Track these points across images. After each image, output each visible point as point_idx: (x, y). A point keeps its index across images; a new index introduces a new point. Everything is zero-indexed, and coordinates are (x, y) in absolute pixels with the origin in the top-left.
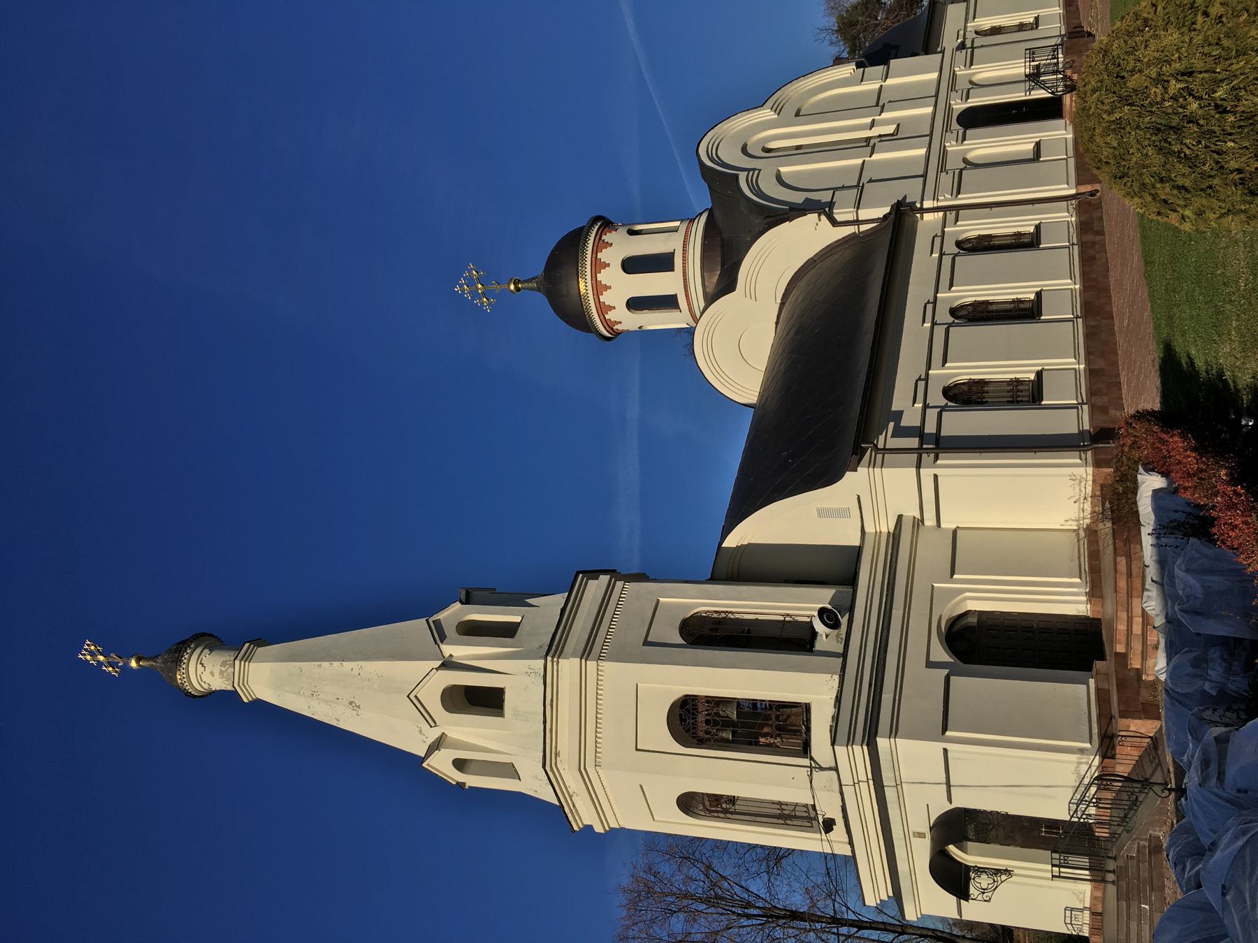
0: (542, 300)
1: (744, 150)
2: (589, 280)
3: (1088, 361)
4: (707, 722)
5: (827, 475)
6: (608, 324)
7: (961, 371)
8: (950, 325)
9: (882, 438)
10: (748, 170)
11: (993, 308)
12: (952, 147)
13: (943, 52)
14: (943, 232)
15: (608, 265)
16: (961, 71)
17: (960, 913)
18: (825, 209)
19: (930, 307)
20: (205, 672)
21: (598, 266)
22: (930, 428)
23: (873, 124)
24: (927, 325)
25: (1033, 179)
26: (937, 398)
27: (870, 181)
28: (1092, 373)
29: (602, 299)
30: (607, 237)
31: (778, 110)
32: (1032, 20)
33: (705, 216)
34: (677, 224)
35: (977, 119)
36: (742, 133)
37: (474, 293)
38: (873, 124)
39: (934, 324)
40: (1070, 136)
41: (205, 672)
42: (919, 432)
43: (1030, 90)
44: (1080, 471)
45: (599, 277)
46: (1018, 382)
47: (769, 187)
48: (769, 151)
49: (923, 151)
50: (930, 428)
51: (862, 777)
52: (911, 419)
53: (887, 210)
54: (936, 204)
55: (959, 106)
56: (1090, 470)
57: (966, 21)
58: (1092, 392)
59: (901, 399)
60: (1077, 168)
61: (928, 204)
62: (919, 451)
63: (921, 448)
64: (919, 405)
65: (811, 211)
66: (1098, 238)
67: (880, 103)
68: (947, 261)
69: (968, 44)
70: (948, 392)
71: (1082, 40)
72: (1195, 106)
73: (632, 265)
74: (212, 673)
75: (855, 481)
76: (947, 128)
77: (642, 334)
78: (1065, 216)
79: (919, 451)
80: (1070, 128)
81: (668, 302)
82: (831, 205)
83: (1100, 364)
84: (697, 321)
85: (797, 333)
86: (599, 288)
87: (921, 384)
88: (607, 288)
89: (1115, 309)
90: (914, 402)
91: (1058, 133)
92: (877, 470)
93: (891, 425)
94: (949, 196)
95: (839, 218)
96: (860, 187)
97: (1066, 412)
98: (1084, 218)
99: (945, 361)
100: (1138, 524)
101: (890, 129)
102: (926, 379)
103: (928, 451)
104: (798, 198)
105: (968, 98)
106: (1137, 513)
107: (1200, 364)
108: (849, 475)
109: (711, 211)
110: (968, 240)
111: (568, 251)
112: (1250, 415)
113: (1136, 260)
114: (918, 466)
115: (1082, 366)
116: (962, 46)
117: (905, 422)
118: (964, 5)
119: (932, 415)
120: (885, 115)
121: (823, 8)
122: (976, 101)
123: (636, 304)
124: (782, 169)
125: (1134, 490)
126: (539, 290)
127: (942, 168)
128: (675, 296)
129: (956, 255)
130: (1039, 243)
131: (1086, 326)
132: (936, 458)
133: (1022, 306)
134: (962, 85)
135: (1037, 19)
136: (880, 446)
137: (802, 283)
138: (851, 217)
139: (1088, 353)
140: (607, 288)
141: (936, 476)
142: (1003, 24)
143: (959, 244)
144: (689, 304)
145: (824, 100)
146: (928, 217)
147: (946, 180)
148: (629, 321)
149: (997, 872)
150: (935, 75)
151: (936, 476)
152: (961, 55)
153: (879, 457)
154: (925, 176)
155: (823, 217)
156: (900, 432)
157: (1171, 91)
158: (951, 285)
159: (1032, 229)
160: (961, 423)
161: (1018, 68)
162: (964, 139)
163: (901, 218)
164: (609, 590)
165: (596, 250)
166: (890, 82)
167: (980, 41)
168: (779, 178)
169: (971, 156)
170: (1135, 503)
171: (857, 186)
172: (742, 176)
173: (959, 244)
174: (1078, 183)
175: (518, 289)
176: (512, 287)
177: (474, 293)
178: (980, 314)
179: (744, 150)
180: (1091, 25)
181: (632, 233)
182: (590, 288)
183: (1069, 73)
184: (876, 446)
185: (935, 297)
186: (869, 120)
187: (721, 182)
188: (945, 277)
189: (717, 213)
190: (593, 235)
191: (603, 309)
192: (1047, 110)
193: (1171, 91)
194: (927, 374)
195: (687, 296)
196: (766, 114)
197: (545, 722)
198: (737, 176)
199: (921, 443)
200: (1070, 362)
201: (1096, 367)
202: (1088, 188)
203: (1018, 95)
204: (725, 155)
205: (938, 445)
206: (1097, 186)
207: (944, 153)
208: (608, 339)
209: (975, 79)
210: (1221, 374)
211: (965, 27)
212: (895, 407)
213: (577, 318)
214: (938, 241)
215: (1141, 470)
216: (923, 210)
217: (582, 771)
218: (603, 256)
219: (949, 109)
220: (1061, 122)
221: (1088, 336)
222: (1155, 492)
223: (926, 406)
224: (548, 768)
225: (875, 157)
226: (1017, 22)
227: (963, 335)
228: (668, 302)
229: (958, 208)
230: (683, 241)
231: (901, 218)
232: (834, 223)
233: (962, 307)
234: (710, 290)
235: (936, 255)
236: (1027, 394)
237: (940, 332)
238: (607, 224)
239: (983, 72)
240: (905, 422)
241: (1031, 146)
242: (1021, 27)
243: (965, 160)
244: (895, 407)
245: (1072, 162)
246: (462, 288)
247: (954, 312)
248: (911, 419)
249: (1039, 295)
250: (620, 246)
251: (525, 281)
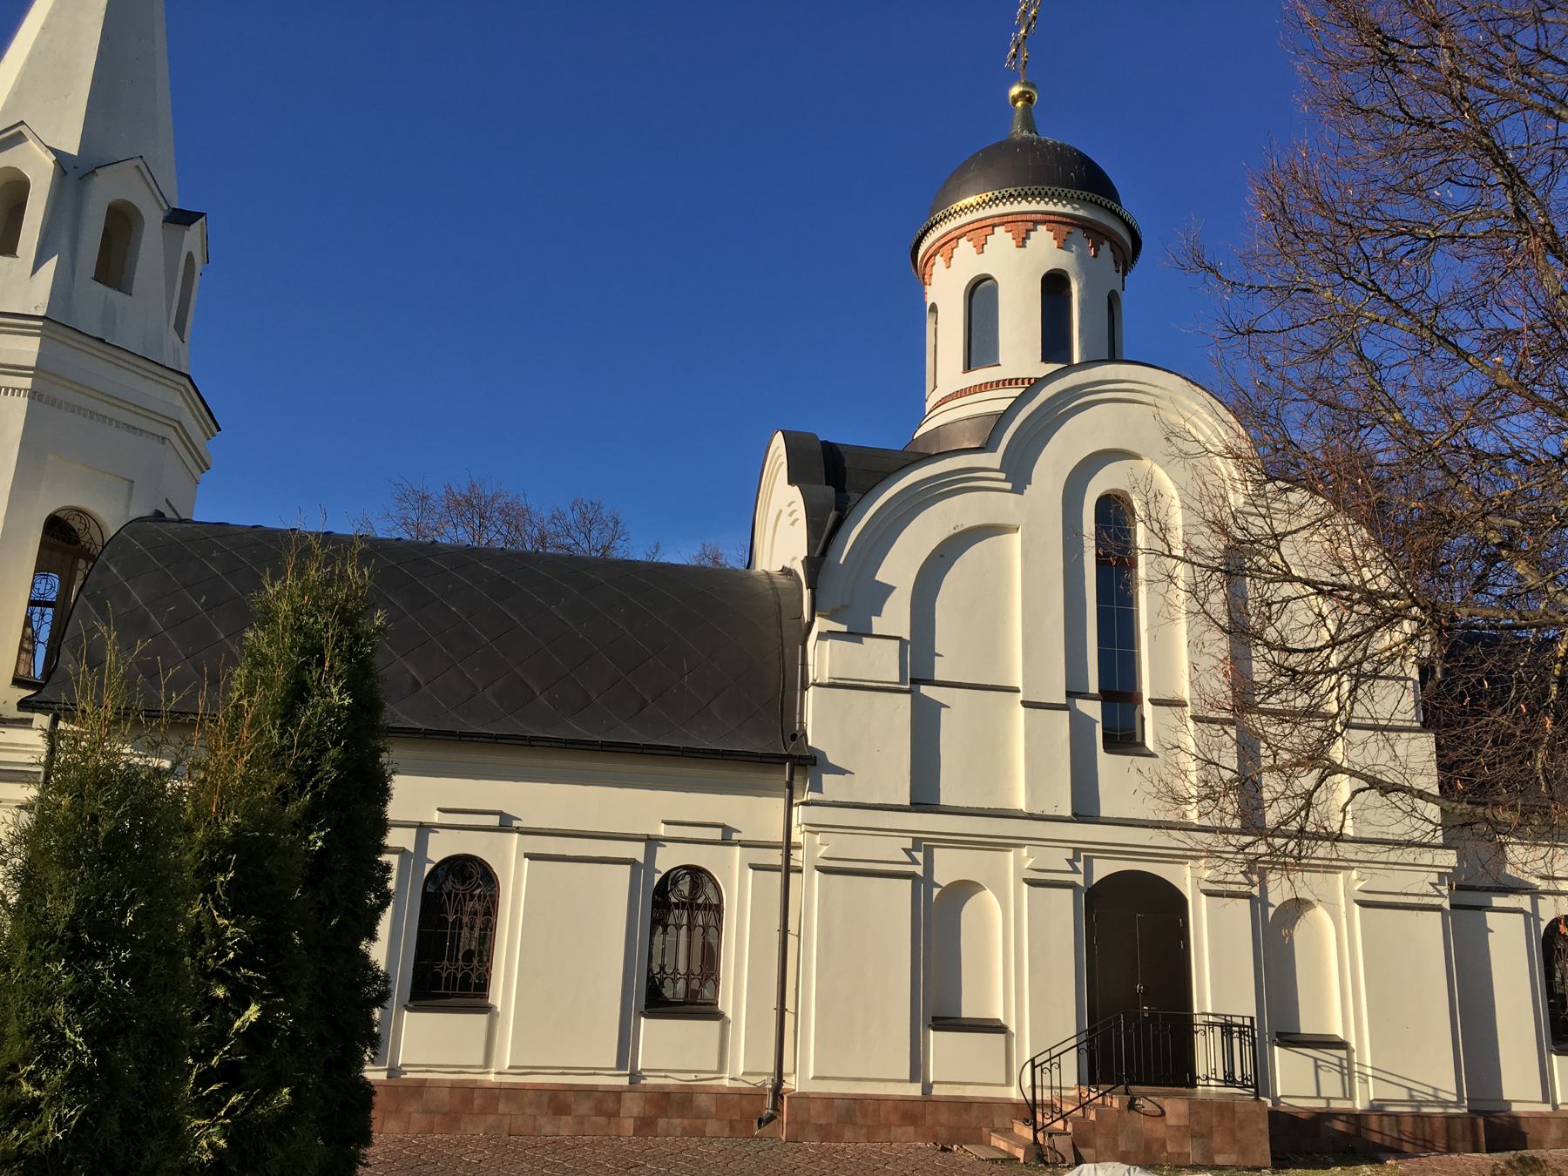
12: (1017, 862)
15: (980, 249)
16: (1344, 885)
23: (1154, 702)
43: (1227, 1028)
55: (1185, 878)
61: (798, 813)
66: (629, 1125)
73: (981, 294)
78: (744, 1065)
82: (858, 633)
94: (823, 851)
98: (703, 1101)
104: (899, 567)
105: (1209, 893)
124: (1016, 539)
147: (891, 850)
159: (726, 1003)
163: (792, 763)
164: (16, 370)
165: (1006, 221)
172: (993, 460)
186: (1185, 693)
188: (555, 849)
190: (1034, 206)
218: (1002, 238)
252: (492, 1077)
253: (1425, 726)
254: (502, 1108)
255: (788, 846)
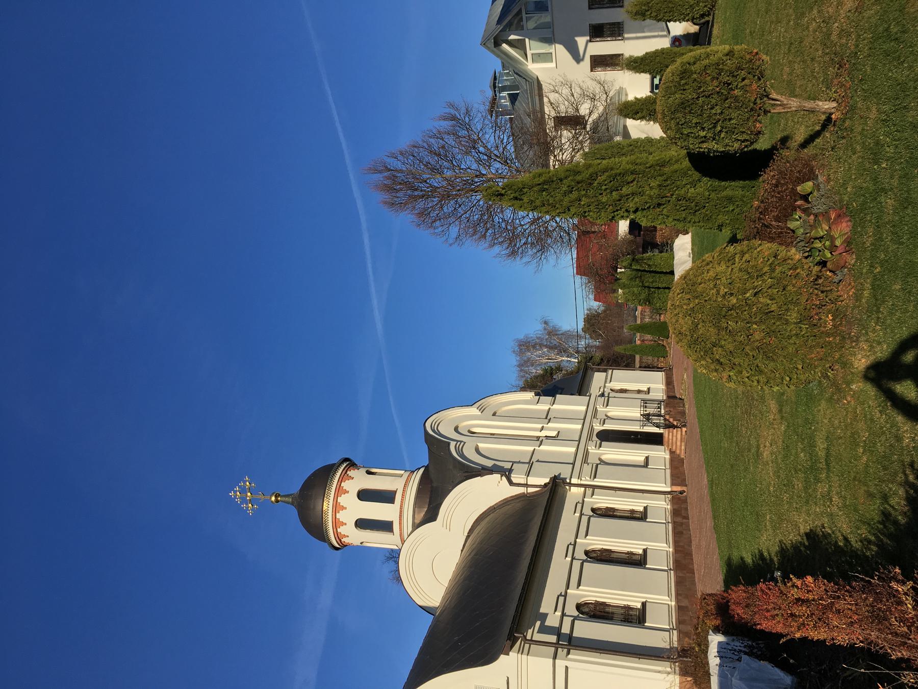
0: (293, 512)
1: (456, 429)
2: (331, 501)
3: (677, 600)
5: (485, 657)
6: (338, 537)
7: (590, 594)
8: (584, 561)
9: (530, 631)
10: (457, 441)
11: (614, 555)
12: (592, 450)
13: (590, 396)
14: (583, 501)
15: (346, 492)
16: (600, 408)
18: (506, 473)
19: (571, 547)
21: (340, 491)
22: (566, 630)
23: (542, 429)
24: (569, 559)
25: (643, 479)
26: (571, 610)
27: (538, 461)
28: (680, 609)
29: (338, 516)
30: (351, 473)
31: (482, 410)
32: (646, 389)
33: (422, 470)
34: (402, 472)
35: (607, 436)
36: (455, 421)
37: (244, 500)
38: (542, 429)
39: (573, 558)
40: (668, 457)
42: (557, 631)
44: (671, 677)
45: (339, 499)
46: (628, 608)
47: (470, 453)
48: (470, 432)
49: (573, 450)
50: (566, 630)
52: (553, 621)
53: (547, 480)
54: (579, 482)
55: (598, 428)
56: (677, 678)
57: (606, 382)
58: (680, 622)
59: (547, 605)
60: (672, 475)
61: (574, 481)
62: (556, 645)
63: (557, 643)
64: (559, 614)
65: (497, 472)
67: (548, 417)
68: (585, 519)
69: (606, 394)
70: (579, 607)
71: (676, 401)
72: (735, 301)
73: (365, 495)
75: (507, 663)
76: (590, 438)
77: (362, 550)
79: (556, 645)
80: (668, 452)
81: (387, 526)
82: (510, 471)
83: (685, 603)
84: (403, 542)
85: (476, 555)
86: (337, 508)
87: (561, 599)
88: (343, 508)
89: (696, 567)
90: (556, 610)
91: (659, 454)
92: (524, 657)
93: (538, 623)
95: (514, 480)
96: (530, 464)
97: (660, 631)
98: (676, 507)
99: (579, 585)
100: (708, 675)
101: (554, 434)
102: (565, 596)
103: (563, 646)
104: (489, 464)
106: (708, 664)
107: (749, 560)
108: (502, 656)
109: (427, 468)
110: (599, 509)
111: (321, 479)
112: (778, 570)
113: (709, 523)
114: (555, 657)
115: (673, 603)
116: (603, 395)
117: (548, 623)
118: (605, 374)
119: (567, 621)
120: (550, 425)
121: (516, 375)
122: (608, 427)
123: (362, 524)
124: (481, 445)
125: (707, 646)
126: (292, 504)
127: (585, 460)
128: (392, 522)
129: (590, 516)
130: (646, 517)
131: (677, 576)
132: (568, 653)
133: (634, 557)
134: (600, 416)
135: (649, 389)
136: (529, 637)
137: (483, 524)
138: (523, 481)
139: (677, 595)
140: (343, 508)
141: (567, 668)
142: (628, 388)
143: (593, 510)
144: (400, 530)
145: (512, 410)
146: (574, 489)
147: (587, 469)
148: (354, 536)
150: (584, 408)
151: (567, 668)
152: (601, 400)
153: (527, 646)
154: (573, 464)
155: (504, 478)
156: (544, 630)
157: (722, 293)
158: (587, 535)
159: (641, 509)
160: (587, 629)
161: (636, 412)
162: (600, 446)
163: (556, 487)
165: (341, 480)
166: (555, 406)
167: (612, 394)
168: (477, 450)
169: (604, 457)
170: (707, 657)
171: (528, 463)
172: (453, 444)
173: (593, 510)
174: (673, 484)
175: (277, 501)
176: (273, 498)
177: (244, 500)
178: (604, 557)
179: (456, 429)
180: (681, 394)
181: (369, 473)
182: (331, 506)
183: (667, 417)
184: (525, 637)
185: (575, 542)
186: (540, 426)
187: (437, 446)
189: (430, 469)
191: (337, 524)
192: (655, 440)
193: (722, 293)
194: (566, 593)
195: (400, 523)
196: (473, 411)
198: (449, 444)
199: (558, 640)
200: (665, 599)
201: (683, 604)
202: (678, 489)
203: (636, 428)
204: (442, 430)
205: (569, 643)
206: (684, 488)
207: (586, 454)
208: (337, 549)
209: (609, 414)
210: (761, 554)
211: (605, 387)
212: (542, 610)
213: (316, 529)
214: (579, 506)
215: (711, 632)
216: (570, 484)
218: (346, 485)
219: (592, 429)
220: (662, 447)
221: (678, 583)
222: (719, 643)
223: (563, 615)
225: (542, 447)
226: (636, 389)
227: (592, 568)
228: (387, 526)
229: (594, 487)
230: (404, 484)
231: (556, 487)
232: (511, 483)
233: (594, 551)
234: (417, 521)
235: (577, 515)
236: (635, 617)
237: (577, 564)
238: (352, 465)
239: (613, 411)
240: (548, 623)
241: (643, 459)
242: (639, 392)
243: (600, 459)
244: (542, 610)
245: (668, 472)
246: (235, 494)
247: (587, 553)
248: (553, 621)
249: (645, 551)
250: (359, 480)
251: (282, 496)
252: (671, 550)
253: (553, 395)
254: (681, 544)
255: (585, 486)
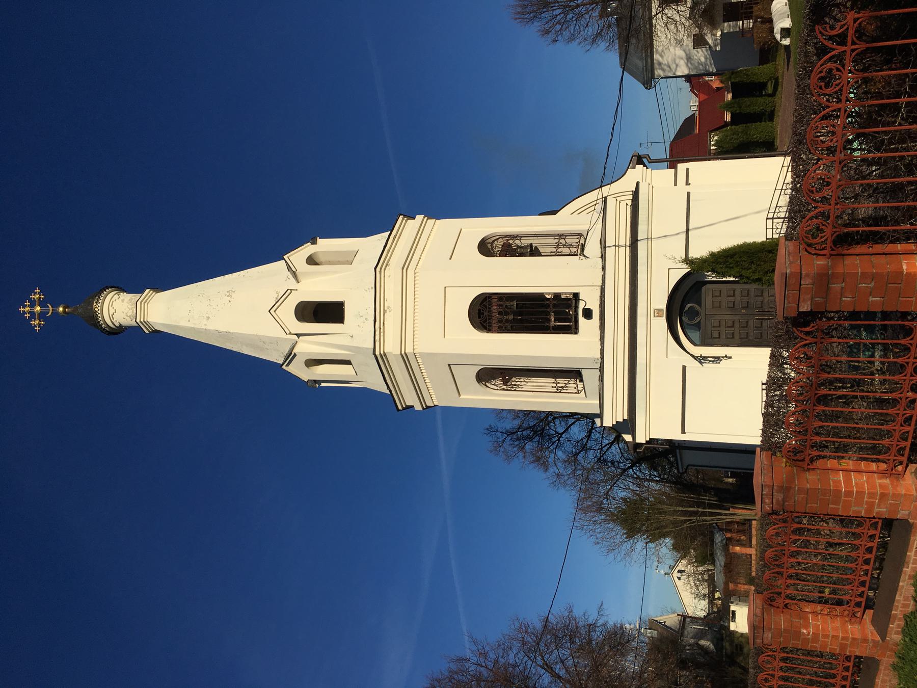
4: (500, 313)
17: (683, 432)
20: (117, 308)
41: (117, 308)
51: (622, 242)
74: (123, 301)
141: (688, 169)
149: (717, 359)
151: (688, 169)
197: (385, 247)
217: (405, 267)
224: (378, 269)
